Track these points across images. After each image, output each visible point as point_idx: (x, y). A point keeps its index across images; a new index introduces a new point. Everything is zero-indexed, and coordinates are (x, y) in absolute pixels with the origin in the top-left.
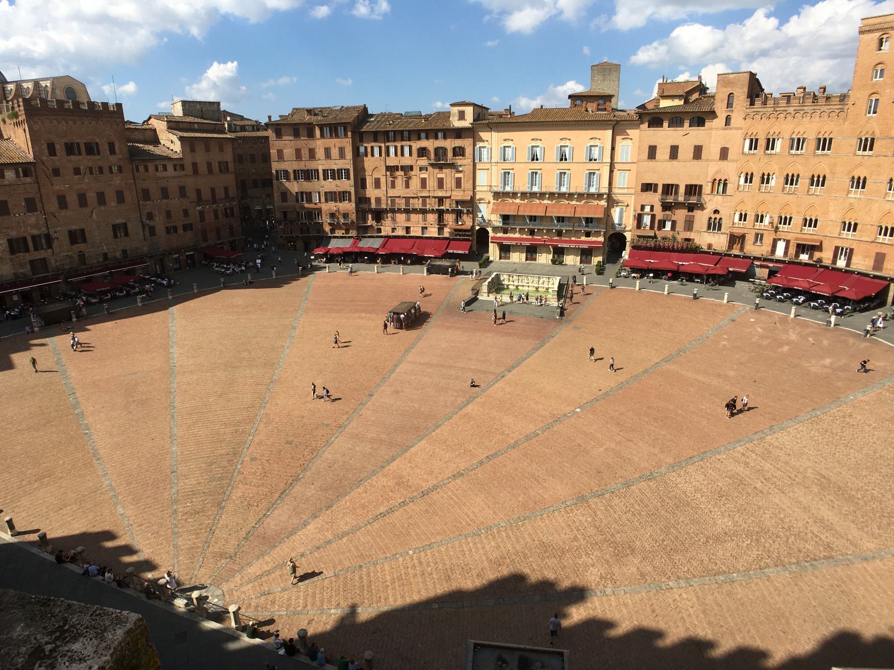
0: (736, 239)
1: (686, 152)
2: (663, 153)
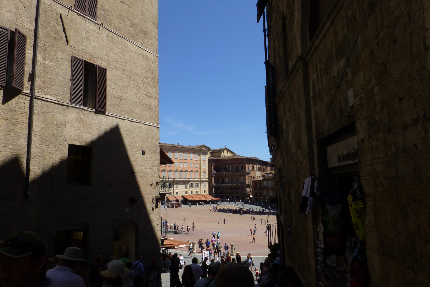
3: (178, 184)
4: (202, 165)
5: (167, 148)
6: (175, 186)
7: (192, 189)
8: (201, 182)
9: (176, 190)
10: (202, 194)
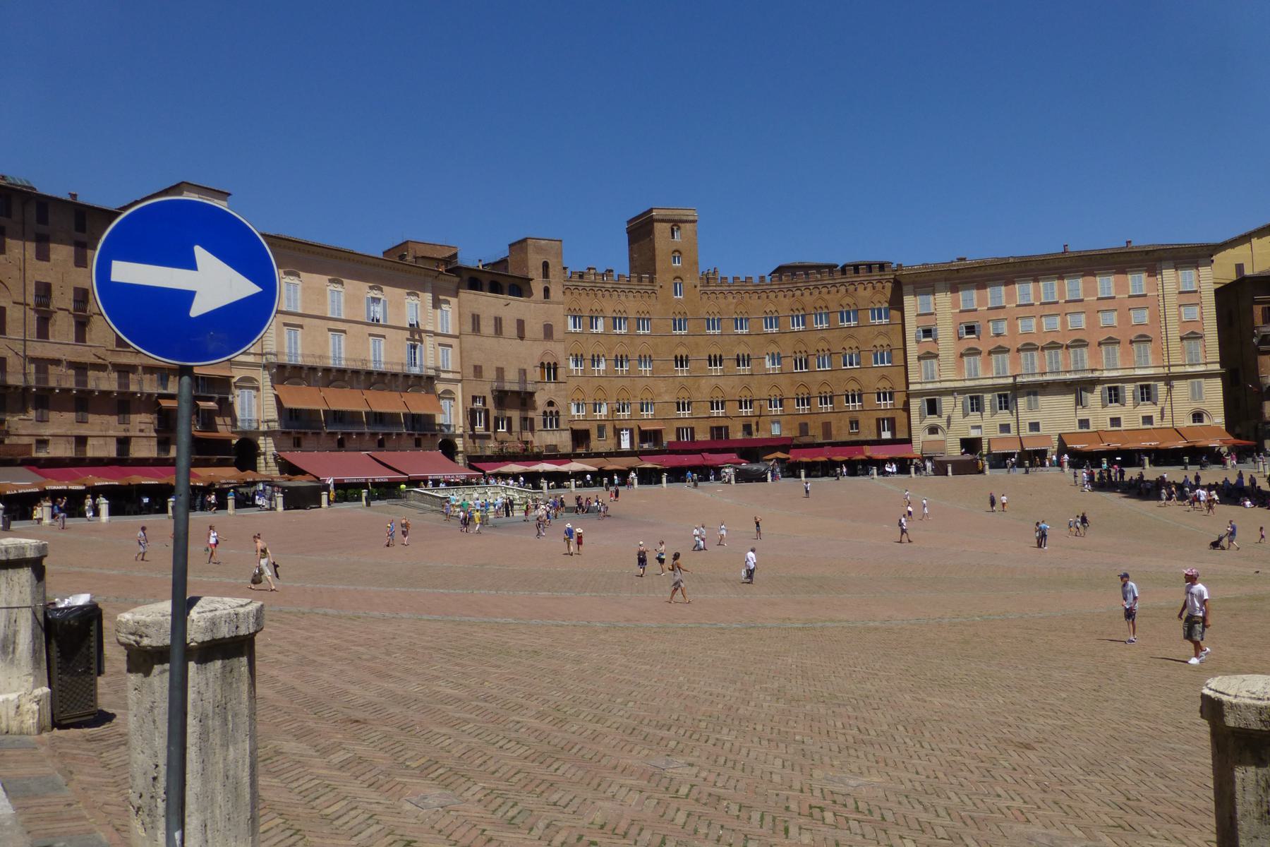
0: (580, 437)
1: (510, 328)
2: (487, 327)
3: (1035, 394)
4: (1172, 312)
5: (989, 271)
6: (1022, 402)
7: (1114, 410)
8: (1169, 379)
9: (1026, 417)
10: (1178, 425)
